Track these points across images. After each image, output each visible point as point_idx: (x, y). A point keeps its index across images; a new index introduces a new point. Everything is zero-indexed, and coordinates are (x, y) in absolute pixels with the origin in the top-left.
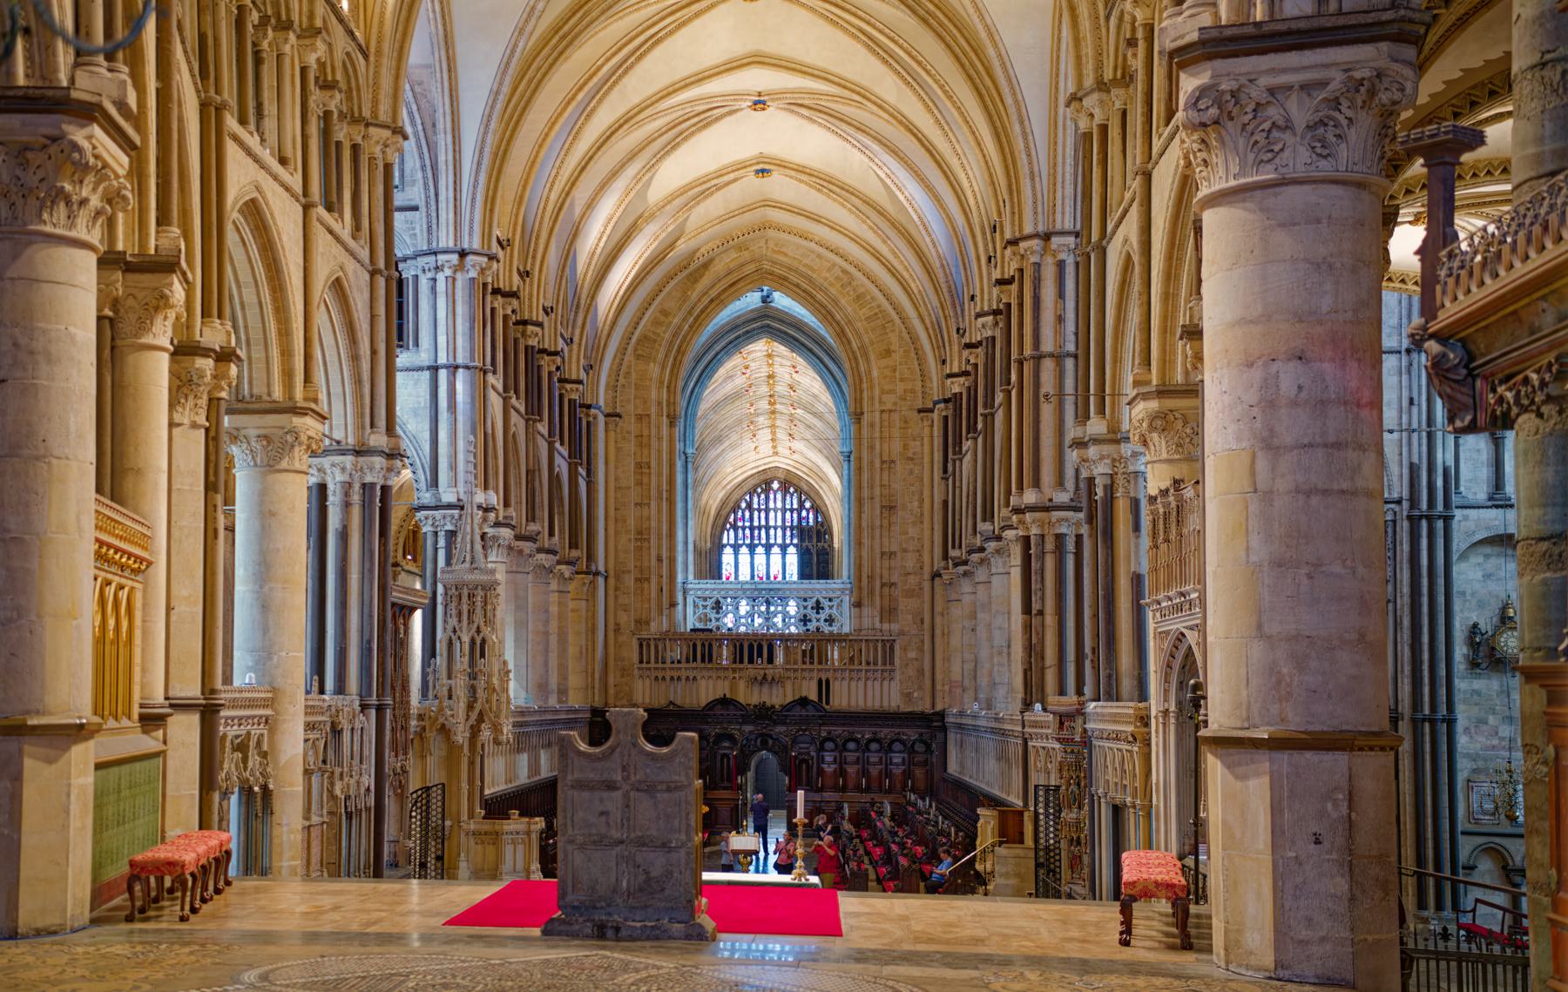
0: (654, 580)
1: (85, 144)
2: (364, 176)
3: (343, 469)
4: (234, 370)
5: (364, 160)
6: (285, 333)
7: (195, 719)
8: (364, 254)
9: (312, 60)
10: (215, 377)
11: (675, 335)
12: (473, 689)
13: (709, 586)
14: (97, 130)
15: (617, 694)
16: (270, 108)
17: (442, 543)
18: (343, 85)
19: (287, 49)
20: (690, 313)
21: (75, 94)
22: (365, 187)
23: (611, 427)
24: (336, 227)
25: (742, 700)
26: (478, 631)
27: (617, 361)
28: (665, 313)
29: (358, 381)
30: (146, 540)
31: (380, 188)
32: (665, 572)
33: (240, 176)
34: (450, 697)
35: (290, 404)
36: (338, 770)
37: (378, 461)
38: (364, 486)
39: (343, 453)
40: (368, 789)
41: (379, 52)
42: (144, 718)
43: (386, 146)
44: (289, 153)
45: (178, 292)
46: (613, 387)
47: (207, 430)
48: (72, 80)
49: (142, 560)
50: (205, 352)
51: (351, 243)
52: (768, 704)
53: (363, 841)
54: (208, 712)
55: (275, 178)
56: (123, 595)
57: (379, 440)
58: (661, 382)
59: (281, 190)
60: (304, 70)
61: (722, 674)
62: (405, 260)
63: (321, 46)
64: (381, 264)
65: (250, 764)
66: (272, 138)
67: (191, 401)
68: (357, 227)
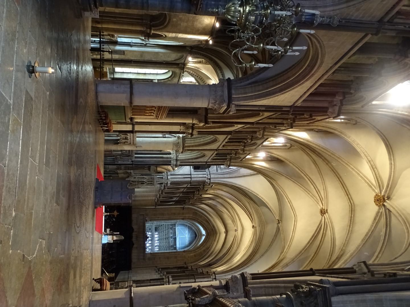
0: (155, 217)
1: (223, 105)
2: (222, 161)
3: (173, 157)
4: (190, 136)
5: (224, 161)
6: (196, 146)
7: (131, 129)
8: (209, 161)
9: (239, 151)
10: (188, 132)
11: (198, 219)
12: (135, 182)
14: (226, 107)
16: (232, 144)
17: (161, 176)
18: (236, 157)
19: (241, 147)
21: (231, 104)
22: (220, 161)
24: (213, 156)
26: (146, 182)
28: (201, 217)
29: (188, 159)
30: (161, 118)
31: (220, 163)
33: (221, 138)
34: (134, 178)
35: (184, 147)
36: (121, 156)
37: (175, 163)
38: (171, 161)
39: (176, 157)
40: (118, 162)
41: (241, 163)
42: (132, 118)
43: (227, 164)
44: (225, 147)
45: (202, 124)
46: (188, 208)
47: (180, 131)
48: (233, 104)
49: (158, 117)
50: (192, 131)
51: (211, 158)
53: (109, 162)
54: (132, 132)
55: (221, 144)
56: (152, 114)
57: (179, 163)
59: (219, 145)
60: (238, 150)
62: (209, 169)
63: (242, 152)
64: (208, 164)
65: (123, 140)
66: (227, 144)
67: (184, 129)
68: (214, 159)
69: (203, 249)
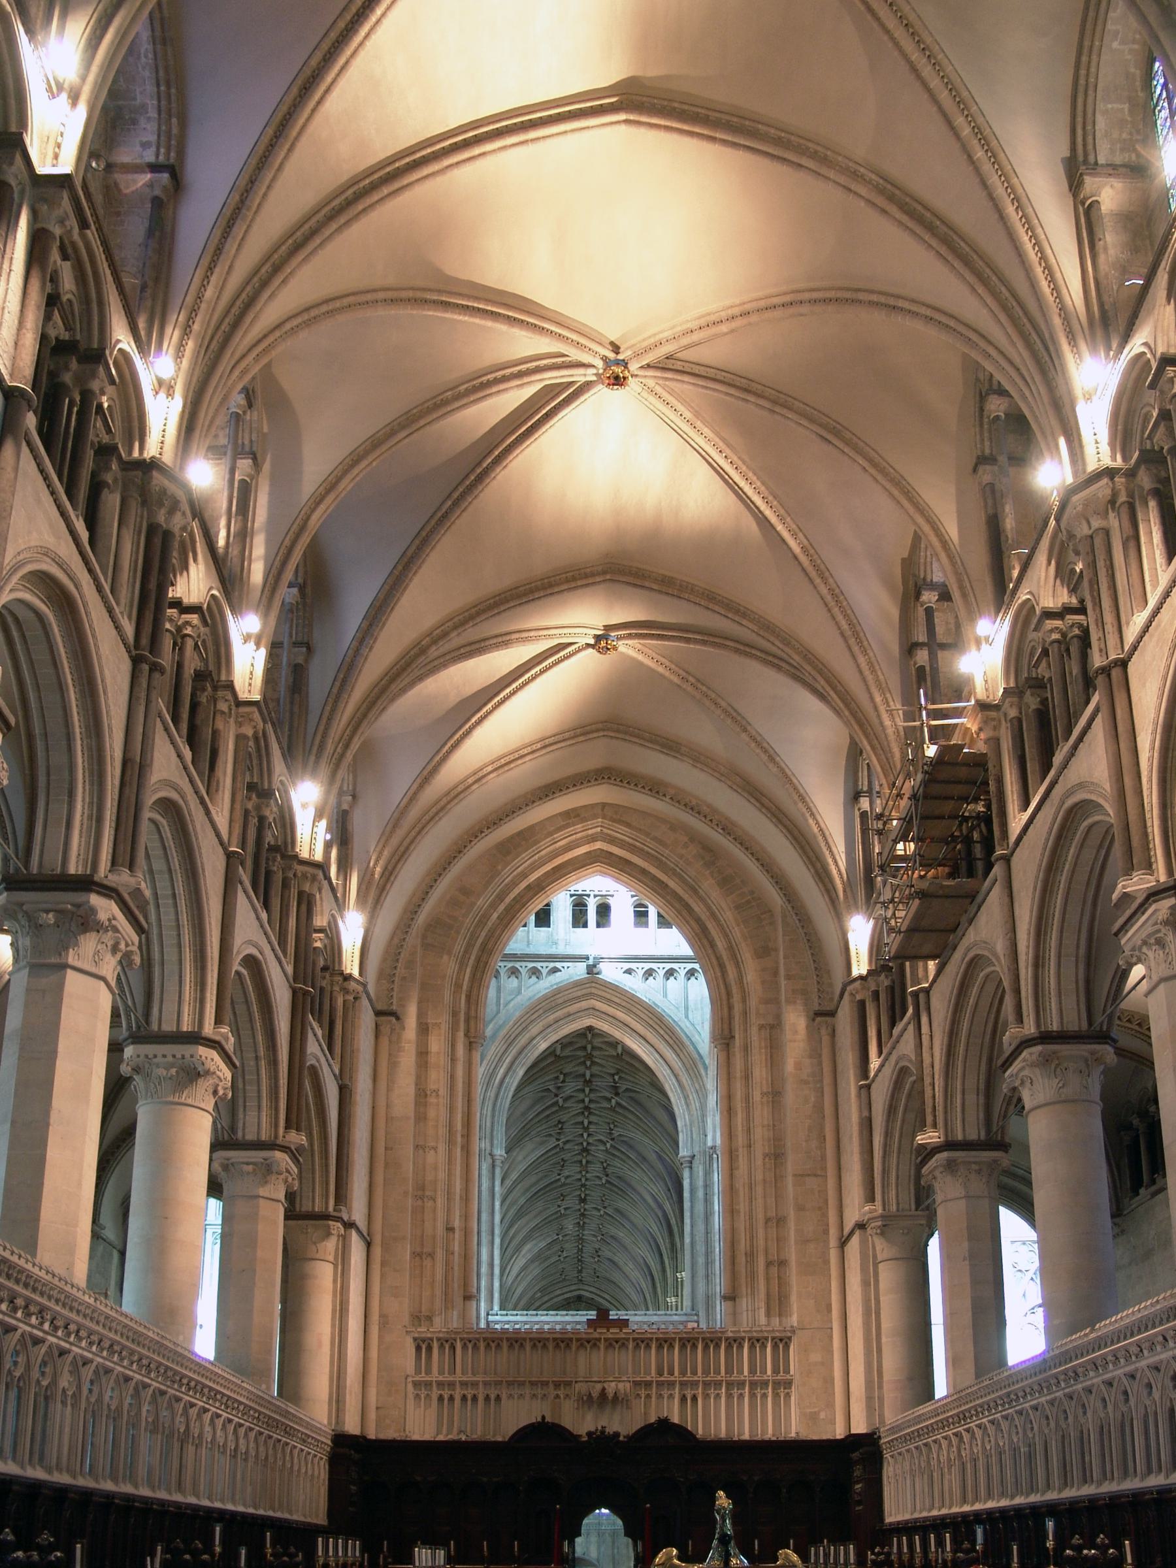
0: (440, 1254)
13: (518, 1318)
15: (379, 1420)
20: (501, 898)
28: (465, 891)
32: (456, 1247)
52: (610, 1430)
58: (458, 986)
61: (539, 1391)
69: (714, 893)
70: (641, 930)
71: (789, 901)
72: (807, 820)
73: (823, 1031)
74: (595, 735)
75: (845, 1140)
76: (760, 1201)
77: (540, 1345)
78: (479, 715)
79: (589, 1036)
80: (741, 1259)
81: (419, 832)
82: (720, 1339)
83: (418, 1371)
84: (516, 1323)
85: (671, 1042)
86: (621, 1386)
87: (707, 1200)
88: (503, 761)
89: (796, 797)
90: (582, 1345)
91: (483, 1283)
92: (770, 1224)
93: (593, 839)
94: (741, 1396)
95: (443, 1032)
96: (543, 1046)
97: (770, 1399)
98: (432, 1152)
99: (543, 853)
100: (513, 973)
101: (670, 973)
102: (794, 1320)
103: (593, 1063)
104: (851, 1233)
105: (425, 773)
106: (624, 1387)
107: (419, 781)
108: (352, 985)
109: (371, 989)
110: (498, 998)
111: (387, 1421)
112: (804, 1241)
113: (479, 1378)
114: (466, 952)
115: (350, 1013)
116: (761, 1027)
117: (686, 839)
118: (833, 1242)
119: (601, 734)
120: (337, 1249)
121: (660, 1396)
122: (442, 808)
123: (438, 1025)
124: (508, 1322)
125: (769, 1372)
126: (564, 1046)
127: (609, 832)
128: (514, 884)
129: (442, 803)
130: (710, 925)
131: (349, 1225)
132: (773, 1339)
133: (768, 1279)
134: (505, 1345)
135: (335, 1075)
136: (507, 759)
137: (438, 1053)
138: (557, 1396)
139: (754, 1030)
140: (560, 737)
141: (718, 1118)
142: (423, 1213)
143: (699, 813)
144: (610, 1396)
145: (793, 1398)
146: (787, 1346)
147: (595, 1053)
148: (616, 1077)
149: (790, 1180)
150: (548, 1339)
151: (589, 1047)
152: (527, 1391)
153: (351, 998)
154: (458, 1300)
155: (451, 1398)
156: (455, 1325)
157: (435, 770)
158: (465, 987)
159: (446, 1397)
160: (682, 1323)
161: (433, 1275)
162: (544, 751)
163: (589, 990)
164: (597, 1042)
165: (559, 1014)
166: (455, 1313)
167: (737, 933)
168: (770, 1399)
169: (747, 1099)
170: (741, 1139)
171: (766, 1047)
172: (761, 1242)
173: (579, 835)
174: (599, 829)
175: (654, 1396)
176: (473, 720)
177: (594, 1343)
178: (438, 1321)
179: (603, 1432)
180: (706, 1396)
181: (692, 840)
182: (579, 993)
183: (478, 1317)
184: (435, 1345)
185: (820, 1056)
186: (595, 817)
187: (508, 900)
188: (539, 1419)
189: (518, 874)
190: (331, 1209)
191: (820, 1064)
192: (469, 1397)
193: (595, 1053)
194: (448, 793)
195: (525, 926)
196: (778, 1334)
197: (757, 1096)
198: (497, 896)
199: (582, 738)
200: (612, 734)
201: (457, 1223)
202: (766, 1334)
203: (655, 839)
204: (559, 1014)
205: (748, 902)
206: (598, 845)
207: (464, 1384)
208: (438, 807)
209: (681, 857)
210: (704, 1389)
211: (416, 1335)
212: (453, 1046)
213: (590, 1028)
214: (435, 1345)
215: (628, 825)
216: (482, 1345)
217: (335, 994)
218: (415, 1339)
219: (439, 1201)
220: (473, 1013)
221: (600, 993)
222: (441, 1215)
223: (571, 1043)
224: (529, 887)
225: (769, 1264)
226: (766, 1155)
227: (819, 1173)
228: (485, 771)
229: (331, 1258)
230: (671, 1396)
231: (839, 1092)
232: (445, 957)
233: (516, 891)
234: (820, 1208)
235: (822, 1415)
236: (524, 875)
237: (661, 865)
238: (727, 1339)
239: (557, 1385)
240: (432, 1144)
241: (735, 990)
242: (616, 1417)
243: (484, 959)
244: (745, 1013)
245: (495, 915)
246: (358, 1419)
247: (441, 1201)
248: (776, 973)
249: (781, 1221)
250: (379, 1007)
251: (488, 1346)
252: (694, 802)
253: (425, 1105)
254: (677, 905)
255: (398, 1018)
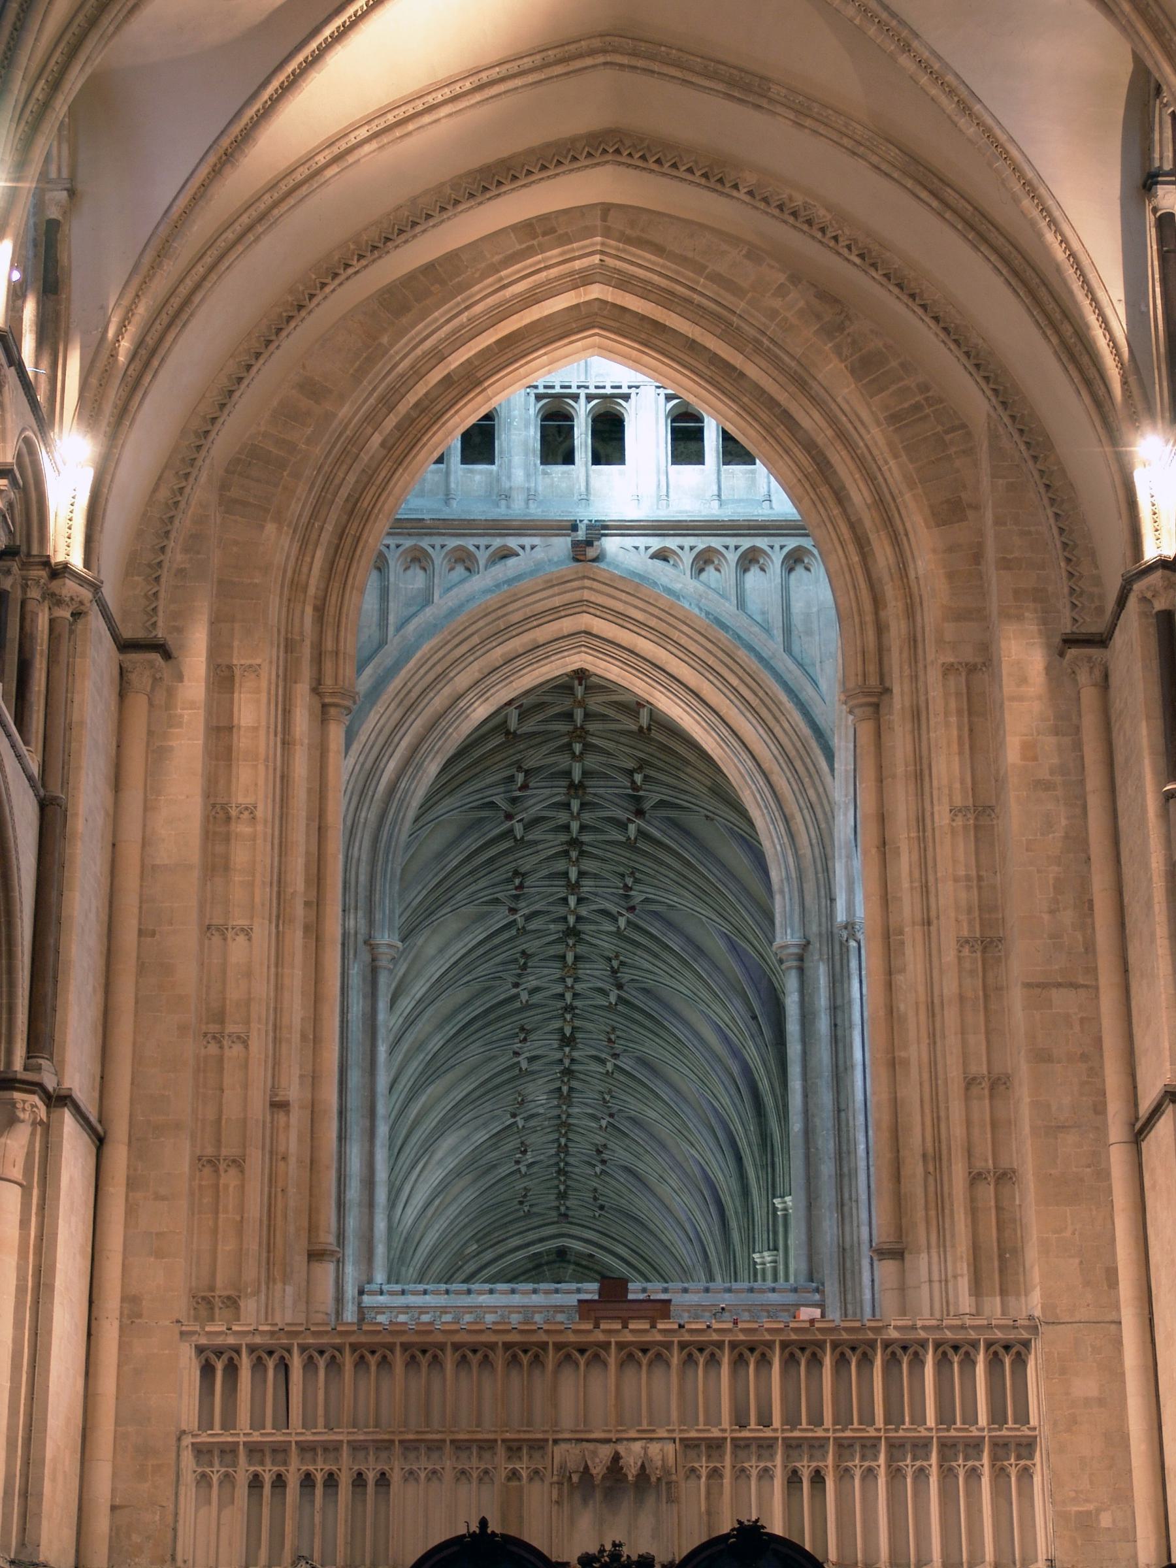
0: (256, 1161)
20: (388, 402)
23: (140, 680)
25: (535, 1535)
27: (164, 494)
28: (313, 389)
52: (630, 1552)
58: (297, 587)
61: (474, 1463)
70: (688, 471)
71: (1004, 404)
72: (1040, 236)
73: (1083, 677)
74: (589, 61)
75: (1134, 910)
76: (952, 1041)
77: (475, 1359)
78: (338, 22)
79: (579, 691)
80: (914, 1168)
81: (212, 268)
82: (872, 1344)
83: (206, 1421)
84: (423, 1310)
85: (754, 701)
86: (654, 1449)
87: (839, 1040)
88: (390, 118)
89: (1017, 187)
90: (568, 1357)
91: (352, 1222)
92: (975, 1090)
93: (584, 279)
94: (921, 1474)
95: (264, 684)
96: (481, 712)
97: (985, 1481)
98: (241, 939)
99: (478, 309)
100: (415, 560)
101: (750, 559)
102: (1034, 1303)
103: (587, 747)
104: (1156, 1112)
105: (225, 142)
106: (662, 1453)
107: (212, 159)
108: (70, 587)
109: (108, 592)
110: (384, 613)
111: (136, 1538)
112: (1051, 1129)
113: (340, 1435)
114: (314, 515)
115: (64, 647)
116: (948, 669)
117: (782, 278)
118: (1116, 1131)
119: (601, 59)
120: (29, 1155)
121: (741, 1473)
122: (262, 218)
123: (254, 669)
124: (407, 1309)
125: (983, 1420)
126: (524, 714)
127: (619, 264)
128: (417, 373)
129: (262, 206)
130: (839, 459)
131: (58, 1100)
132: (989, 1344)
133: (974, 1212)
134: (399, 1360)
135: (30, 778)
136: (400, 114)
137: (256, 729)
138: (514, 1475)
139: (933, 676)
140: (513, 67)
141: (857, 863)
142: (221, 1070)
143: (809, 222)
144: (632, 1472)
145: (1037, 1479)
146: (1020, 1362)
147: (592, 727)
148: (638, 778)
149: (1016, 998)
150: (492, 1346)
151: (579, 714)
152: (448, 1463)
153: (65, 613)
154: (300, 1260)
155: (279, 1482)
156: (288, 1319)
157: (247, 136)
158: (312, 590)
159: (267, 1479)
160: (785, 1307)
161: (241, 1208)
162: (478, 97)
163: (576, 595)
164: (595, 703)
165: (516, 644)
166: (289, 1289)
167: (894, 471)
168: (985, 1481)
169: (921, 821)
170: (908, 907)
171: (959, 712)
172: (958, 1131)
173: (554, 272)
174: (596, 259)
175: (727, 1473)
176: (327, 32)
177: (593, 1353)
178: (250, 1307)
179: (615, 1556)
180: (844, 1474)
181: (795, 279)
182: (557, 601)
183: (339, 1299)
184: (245, 1363)
185: (1078, 729)
186: (588, 232)
187: (403, 408)
188: (474, 1528)
189: (425, 354)
190: (18, 1064)
191: (1078, 746)
192: (319, 1478)
193: (592, 727)
194: (273, 186)
195: (440, 460)
196: (999, 1335)
197: (941, 816)
198: (382, 399)
199: (559, 69)
200: (625, 60)
201: (293, 1092)
202: (973, 1335)
203: (715, 278)
204: (516, 644)
205: (917, 407)
206: (596, 292)
207: (306, 1449)
208: (253, 213)
209: (773, 314)
210: (839, 1457)
211: (203, 1341)
212: (287, 713)
213: (581, 675)
214: (245, 1363)
215: (659, 250)
216: (348, 1360)
217: (31, 606)
218: (200, 1350)
219: (255, 1045)
220: (329, 645)
221: (601, 599)
222: (259, 1075)
223: (540, 706)
224: (448, 381)
225: (975, 1178)
226: (963, 942)
227: (1081, 981)
228: (352, 140)
229: (17, 1173)
230: (766, 1474)
231: (1121, 803)
232: (270, 528)
233: (421, 390)
234: (1084, 1057)
235: (1105, 1520)
236: (438, 356)
237: (729, 332)
238: (887, 1345)
239: (514, 1449)
240: (243, 922)
241: (891, 592)
242: (646, 1521)
243: (352, 530)
244: (913, 641)
245: (377, 439)
246: (68, 1534)
247: (257, 1045)
248: (977, 557)
249: (999, 1084)
250: (127, 633)
251: (361, 1362)
252: (799, 199)
253: (227, 839)
254: (764, 416)
255: (167, 655)
